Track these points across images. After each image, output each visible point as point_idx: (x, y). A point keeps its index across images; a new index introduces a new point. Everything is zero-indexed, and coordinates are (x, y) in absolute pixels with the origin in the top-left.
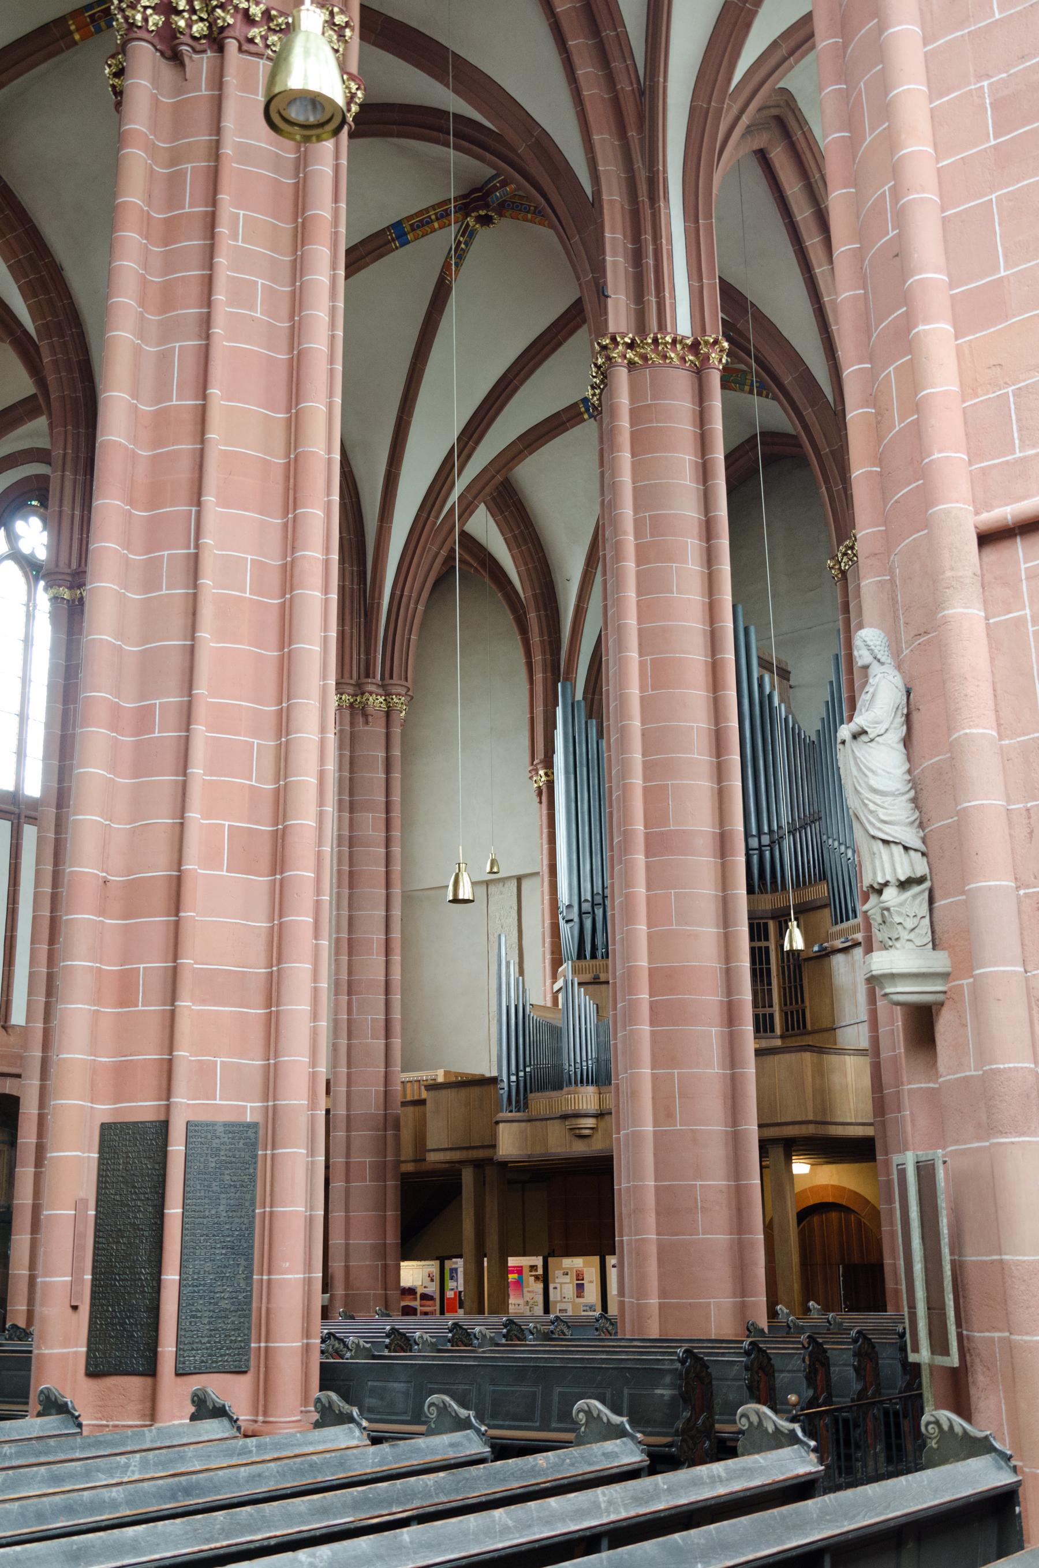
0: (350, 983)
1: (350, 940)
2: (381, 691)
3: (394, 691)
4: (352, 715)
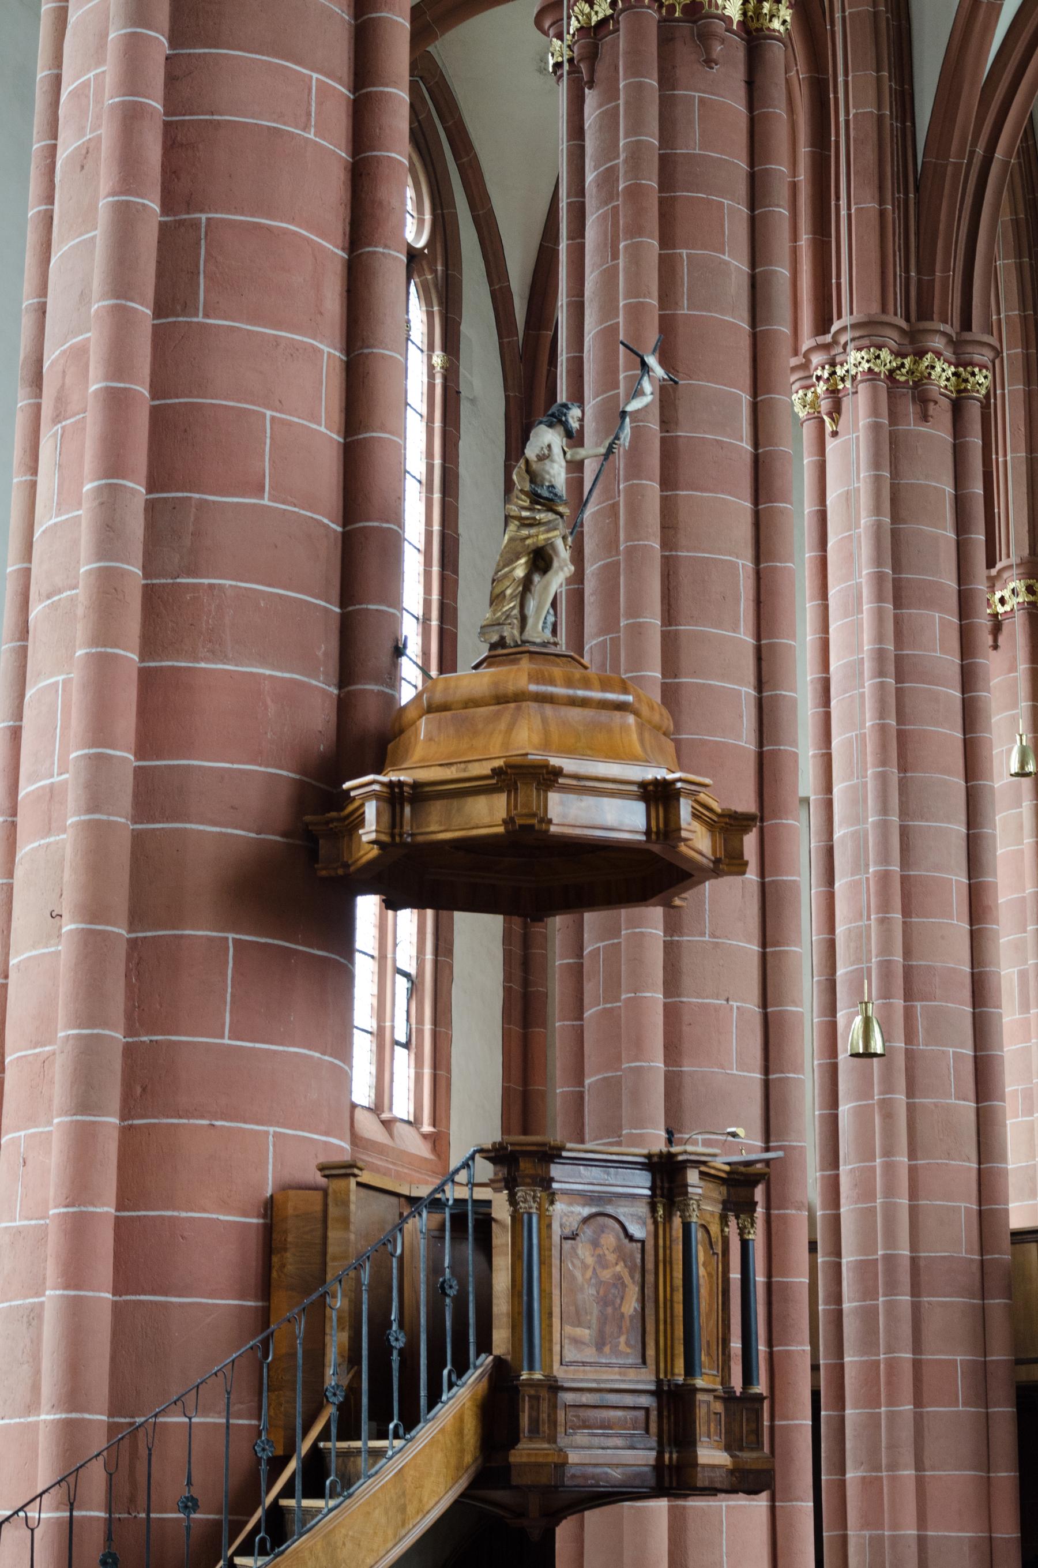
0: (908, 972)
1: (905, 880)
2: (948, 354)
3: (977, 358)
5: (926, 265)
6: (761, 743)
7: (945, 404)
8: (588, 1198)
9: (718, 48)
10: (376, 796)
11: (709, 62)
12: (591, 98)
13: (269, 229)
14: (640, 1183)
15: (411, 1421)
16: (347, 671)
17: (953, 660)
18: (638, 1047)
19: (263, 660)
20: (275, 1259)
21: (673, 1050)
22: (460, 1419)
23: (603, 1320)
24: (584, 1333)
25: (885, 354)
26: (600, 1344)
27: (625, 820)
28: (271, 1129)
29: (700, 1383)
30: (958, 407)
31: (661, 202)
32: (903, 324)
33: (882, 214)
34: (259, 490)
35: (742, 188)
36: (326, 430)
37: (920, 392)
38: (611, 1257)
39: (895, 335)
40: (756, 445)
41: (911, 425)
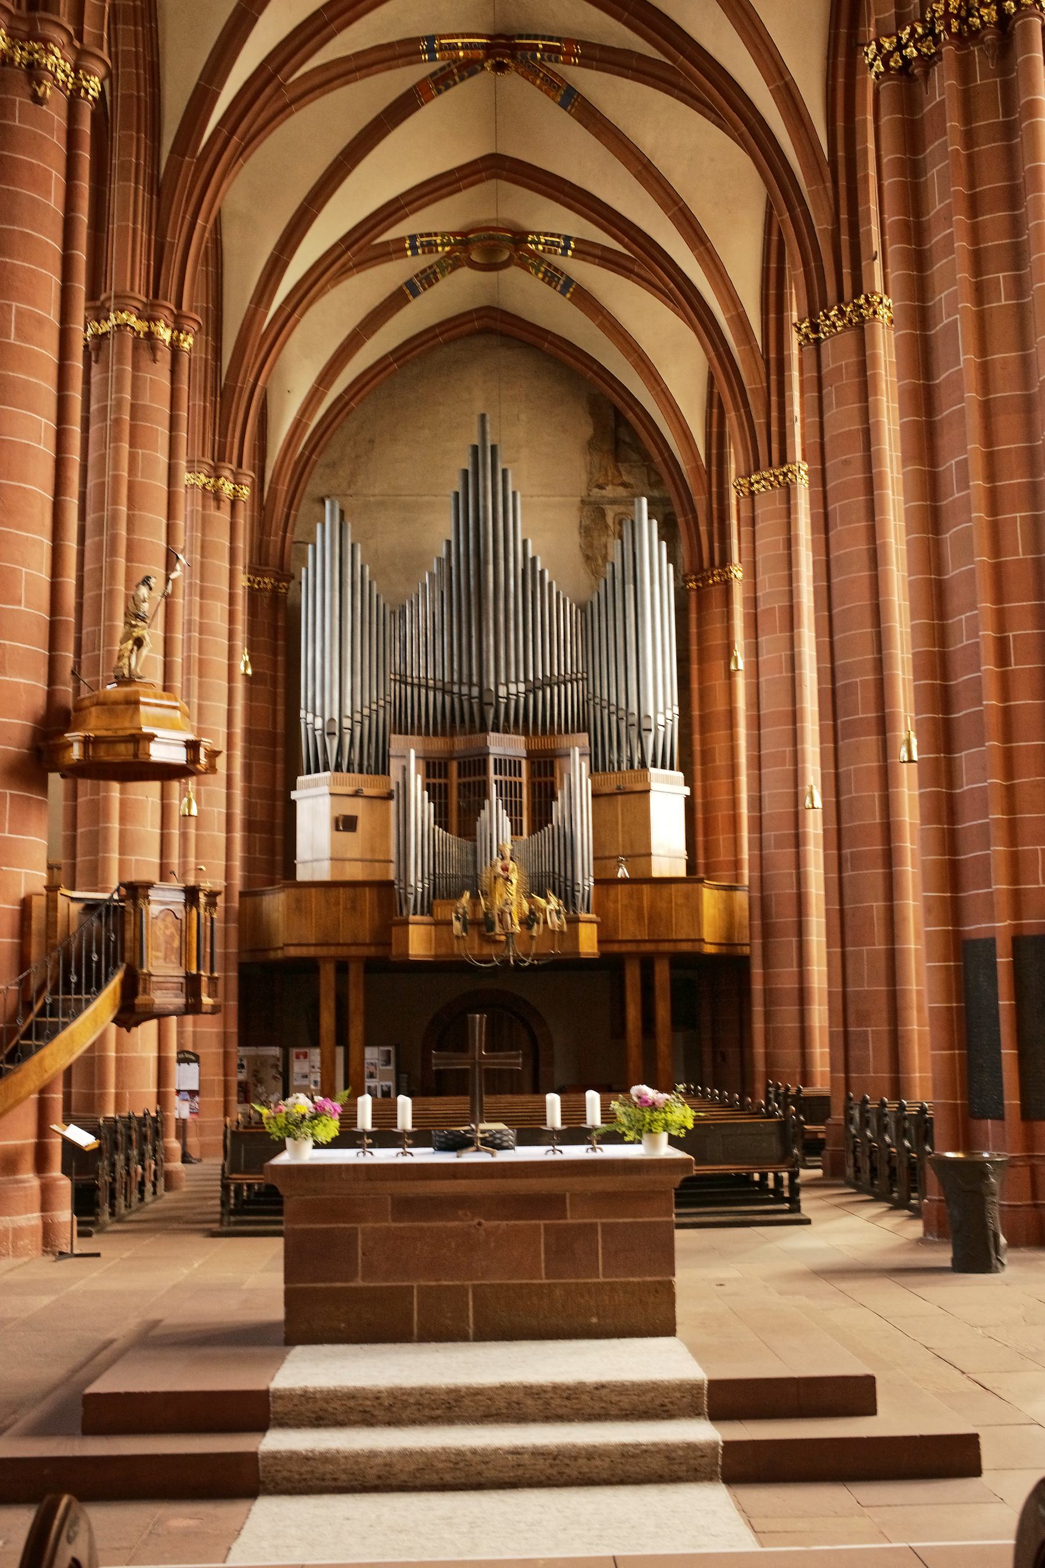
2: (231, 478)
3: (244, 481)
4: (204, 496)
5: (224, 434)
6: (165, 682)
7: (228, 502)
8: (162, 903)
9: (159, 354)
10: (79, 741)
11: (155, 361)
12: (95, 368)
13: (25, 489)
14: (181, 897)
15: (99, 988)
16: (52, 679)
17: (225, 626)
18: (107, 817)
19: (21, 676)
20: (26, 923)
21: (123, 819)
22: (115, 988)
23: (166, 948)
24: (161, 954)
25: (202, 476)
26: (165, 959)
27: (178, 756)
28: (23, 871)
29: (202, 973)
30: (234, 504)
31: (131, 426)
32: (211, 463)
33: (205, 407)
34: (19, 603)
35: (166, 422)
36: (45, 576)
37: (217, 497)
38: (170, 925)
39: (207, 467)
40: (168, 543)
41: (212, 511)
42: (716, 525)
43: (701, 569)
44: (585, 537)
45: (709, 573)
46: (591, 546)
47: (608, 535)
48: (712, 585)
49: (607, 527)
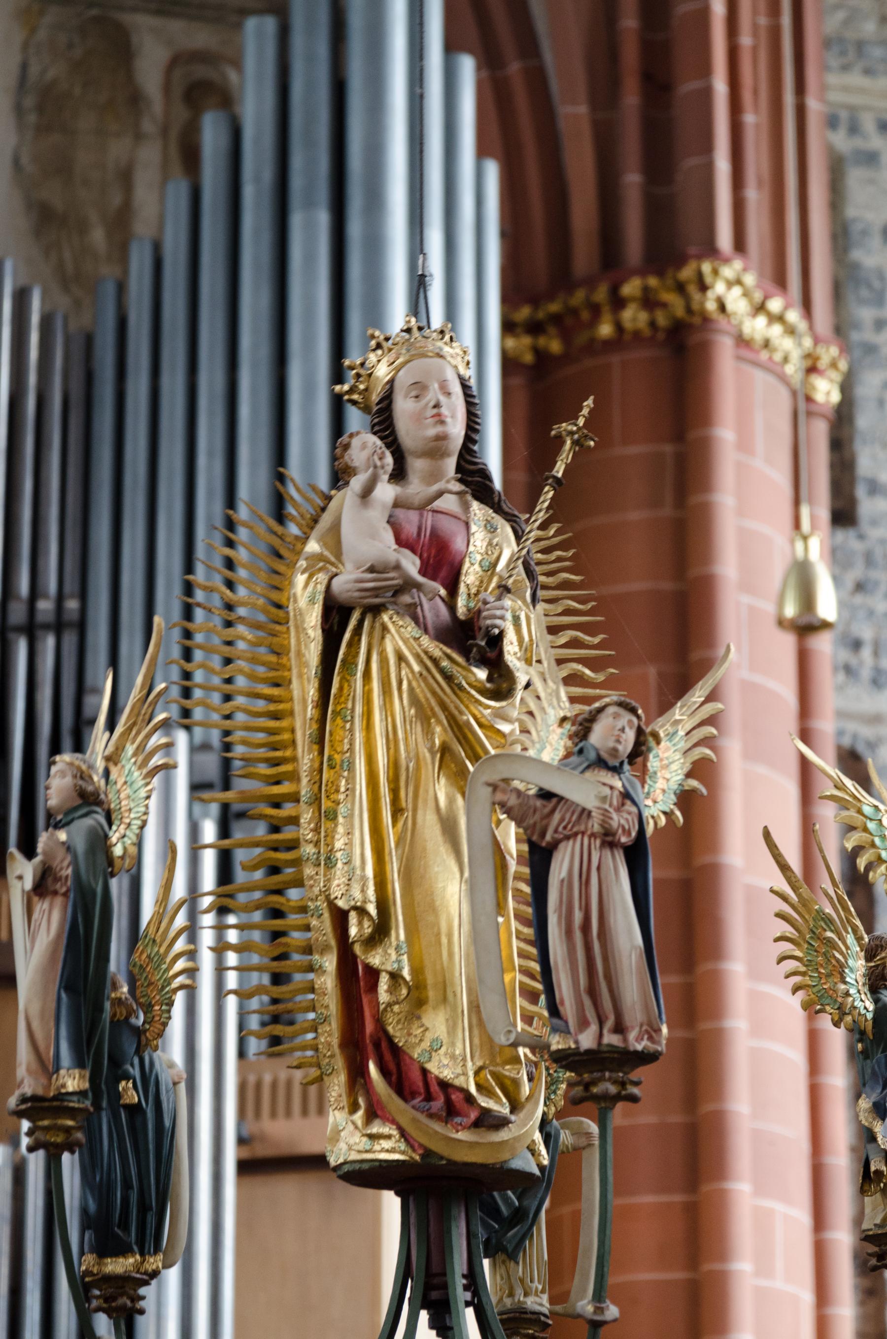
42: (631, 99)
43: (562, 279)
44: (43, 129)
45: (601, 294)
46: (61, 167)
47: (139, 137)
48: (610, 345)
49: (136, 99)
